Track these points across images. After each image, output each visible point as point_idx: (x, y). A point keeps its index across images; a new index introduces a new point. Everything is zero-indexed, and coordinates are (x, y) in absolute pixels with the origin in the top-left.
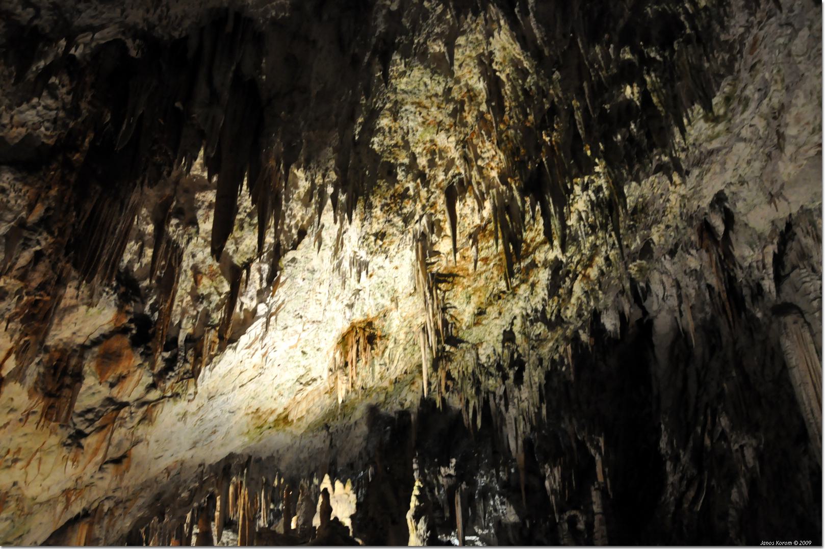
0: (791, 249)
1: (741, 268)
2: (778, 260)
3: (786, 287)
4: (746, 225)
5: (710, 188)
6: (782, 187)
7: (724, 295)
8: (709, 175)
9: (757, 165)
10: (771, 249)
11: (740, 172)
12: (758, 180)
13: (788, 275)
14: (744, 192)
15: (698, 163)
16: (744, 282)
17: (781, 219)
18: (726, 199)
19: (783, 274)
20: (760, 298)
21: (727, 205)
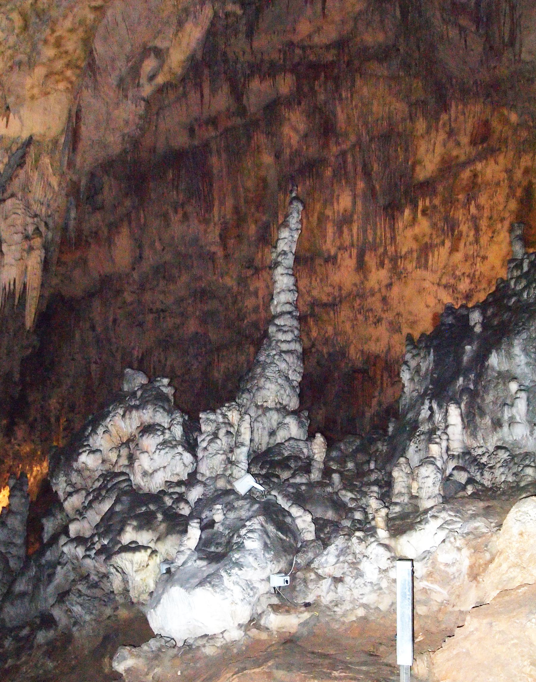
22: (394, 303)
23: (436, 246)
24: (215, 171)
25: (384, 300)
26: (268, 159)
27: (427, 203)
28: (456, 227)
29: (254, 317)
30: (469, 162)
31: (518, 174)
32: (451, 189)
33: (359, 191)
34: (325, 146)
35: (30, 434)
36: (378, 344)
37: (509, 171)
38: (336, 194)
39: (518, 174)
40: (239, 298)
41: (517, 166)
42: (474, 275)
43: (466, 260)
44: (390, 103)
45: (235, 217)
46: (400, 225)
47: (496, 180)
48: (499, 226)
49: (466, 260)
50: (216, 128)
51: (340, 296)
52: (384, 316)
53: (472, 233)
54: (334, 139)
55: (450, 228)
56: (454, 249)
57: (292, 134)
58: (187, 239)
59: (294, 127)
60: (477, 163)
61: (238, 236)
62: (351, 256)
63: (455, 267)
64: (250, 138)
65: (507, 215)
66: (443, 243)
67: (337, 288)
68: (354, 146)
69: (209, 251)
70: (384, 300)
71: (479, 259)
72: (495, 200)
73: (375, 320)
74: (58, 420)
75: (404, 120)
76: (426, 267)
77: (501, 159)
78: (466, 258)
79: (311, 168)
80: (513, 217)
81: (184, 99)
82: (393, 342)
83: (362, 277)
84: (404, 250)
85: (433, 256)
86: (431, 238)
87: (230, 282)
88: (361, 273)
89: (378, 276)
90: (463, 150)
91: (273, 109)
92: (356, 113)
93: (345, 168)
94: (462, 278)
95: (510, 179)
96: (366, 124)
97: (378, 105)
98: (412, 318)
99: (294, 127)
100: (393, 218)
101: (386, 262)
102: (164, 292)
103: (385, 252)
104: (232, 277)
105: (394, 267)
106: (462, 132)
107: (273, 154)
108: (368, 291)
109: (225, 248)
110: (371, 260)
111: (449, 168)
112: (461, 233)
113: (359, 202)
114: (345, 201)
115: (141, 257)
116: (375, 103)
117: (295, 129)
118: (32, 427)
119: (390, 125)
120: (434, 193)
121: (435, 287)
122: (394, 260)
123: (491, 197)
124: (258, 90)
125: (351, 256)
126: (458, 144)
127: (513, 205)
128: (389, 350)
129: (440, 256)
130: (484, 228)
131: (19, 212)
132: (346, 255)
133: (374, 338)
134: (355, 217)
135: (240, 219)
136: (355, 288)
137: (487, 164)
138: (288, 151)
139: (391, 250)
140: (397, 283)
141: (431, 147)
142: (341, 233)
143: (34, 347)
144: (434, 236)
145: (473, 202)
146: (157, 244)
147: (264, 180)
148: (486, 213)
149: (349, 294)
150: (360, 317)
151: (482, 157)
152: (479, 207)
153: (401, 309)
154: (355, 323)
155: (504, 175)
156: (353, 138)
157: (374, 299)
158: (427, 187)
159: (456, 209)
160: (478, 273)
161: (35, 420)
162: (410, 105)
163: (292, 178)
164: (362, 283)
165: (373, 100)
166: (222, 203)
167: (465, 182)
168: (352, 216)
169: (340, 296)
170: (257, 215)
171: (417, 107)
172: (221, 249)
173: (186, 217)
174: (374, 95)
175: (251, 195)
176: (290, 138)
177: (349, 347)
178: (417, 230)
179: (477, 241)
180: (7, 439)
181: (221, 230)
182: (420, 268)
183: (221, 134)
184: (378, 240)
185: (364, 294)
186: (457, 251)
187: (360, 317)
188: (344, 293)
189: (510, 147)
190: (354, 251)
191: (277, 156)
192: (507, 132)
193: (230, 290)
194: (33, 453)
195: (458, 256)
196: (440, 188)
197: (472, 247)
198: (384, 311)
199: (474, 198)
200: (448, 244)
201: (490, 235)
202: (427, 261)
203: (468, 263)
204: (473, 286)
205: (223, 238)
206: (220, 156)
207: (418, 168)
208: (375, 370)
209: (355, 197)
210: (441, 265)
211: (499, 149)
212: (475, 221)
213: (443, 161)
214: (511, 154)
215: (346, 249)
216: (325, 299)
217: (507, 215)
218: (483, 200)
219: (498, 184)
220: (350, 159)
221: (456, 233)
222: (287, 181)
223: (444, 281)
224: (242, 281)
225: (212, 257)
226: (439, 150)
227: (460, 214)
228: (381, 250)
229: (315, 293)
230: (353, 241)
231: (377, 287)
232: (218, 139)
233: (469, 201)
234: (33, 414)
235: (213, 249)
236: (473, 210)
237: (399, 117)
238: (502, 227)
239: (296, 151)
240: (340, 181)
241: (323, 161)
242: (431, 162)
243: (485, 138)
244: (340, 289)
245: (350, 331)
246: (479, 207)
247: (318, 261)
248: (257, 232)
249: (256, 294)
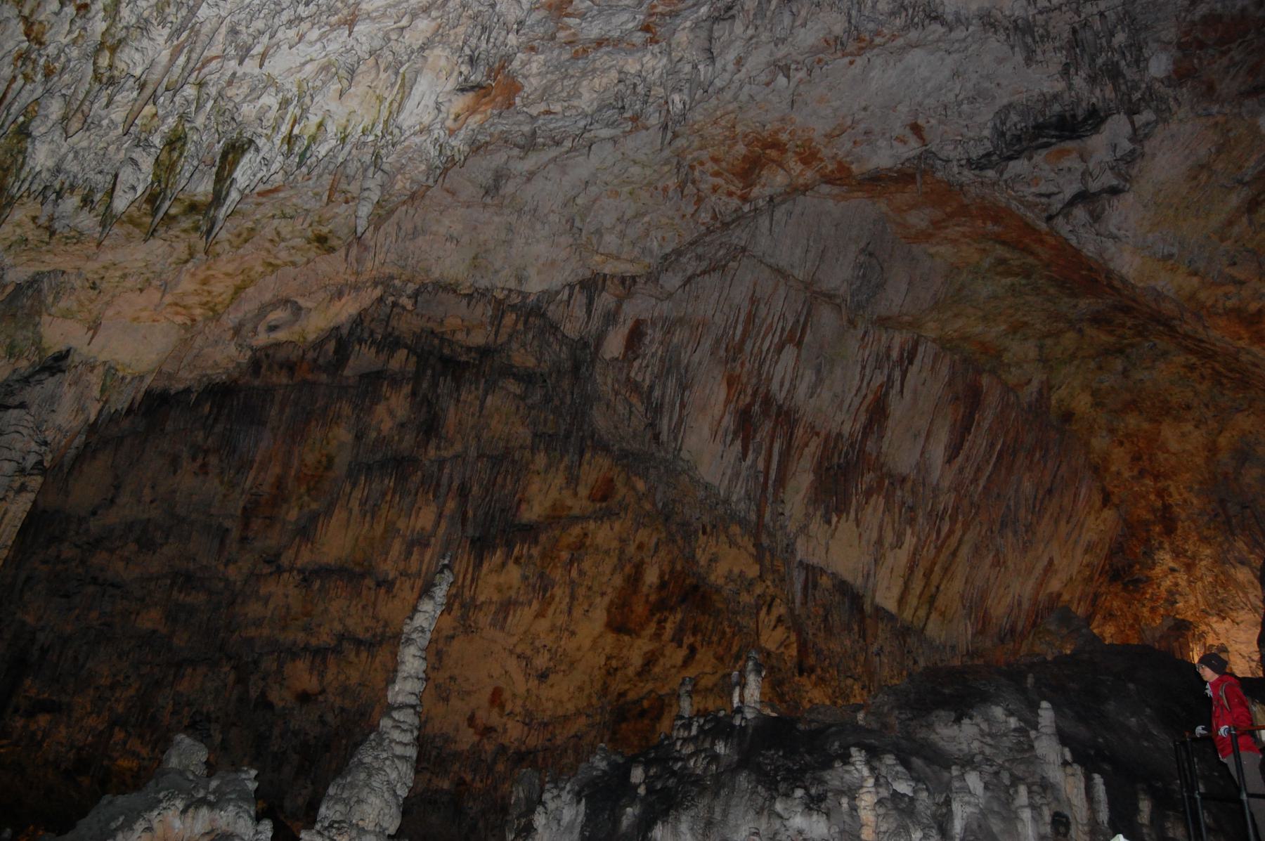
23: (522, 604)
26: (343, 434)
29: (252, 632)
30: (583, 518)
33: (447, 512)
39: (631, 549)
40: (239, 600)
42: (556, 651)
48: (598, 600)
50: (292, 376)
51: (384, 633)
55: (543, 587)
56: (540, 615)
59: (392, 412)
62: (412, 588)
65: (610, 590)
67: (382, 623)
68: (456, 457)
72: (600, 569)
76: (502, 628)
78: (553, 629)
79: (400, 465)
84: (482, 598)
85: (514, 616)
90: (579, 503)
91: (373, 381)
95: (622, 551)
96: (478, 438)
101: (456, 606)
105: (465, 617)
109: (246, 526)
111: (558, 518)
112: (553, 597)
113: (443, 525)
114: (425, 518)
115: (112, 501)
117: (391, 412)
125: (412, 588)
126: (576, 494)
127: (618, 581)
129: (521, 618)
130: (581, 599)
131: (25, 432)
132: (407, 585)
138: (374, 435)
142: (409, 553)
146: (147, 491)
152: (581, 573)
155: (615, 544)
156: (458, 447)
158: (530, 532)
159: (555, 566)
162: (535, 435)
163: (369, 468)
169: (384, 633)
178: (502, 579)
186: (544, 616)
191: (358, 437)
195: (544, 624)
196: (543, 538)
200: (535, 605)
202: (505, 619)
207: (524, 506)
209: (440, 516)
213: (554, 507)
215: (407, 575)
216: (360, 633)
218: (586, 565)
219: (607, 552)
221: (548, 595)
222: (359, 470)
223: (518, 650)
227: (558, 575)
229: (350, 622)
233: (571, 562)
235: (228, 524)
236: (574, 573)
244: (386, 625)
246: (581, 573)
247: (369, 582)
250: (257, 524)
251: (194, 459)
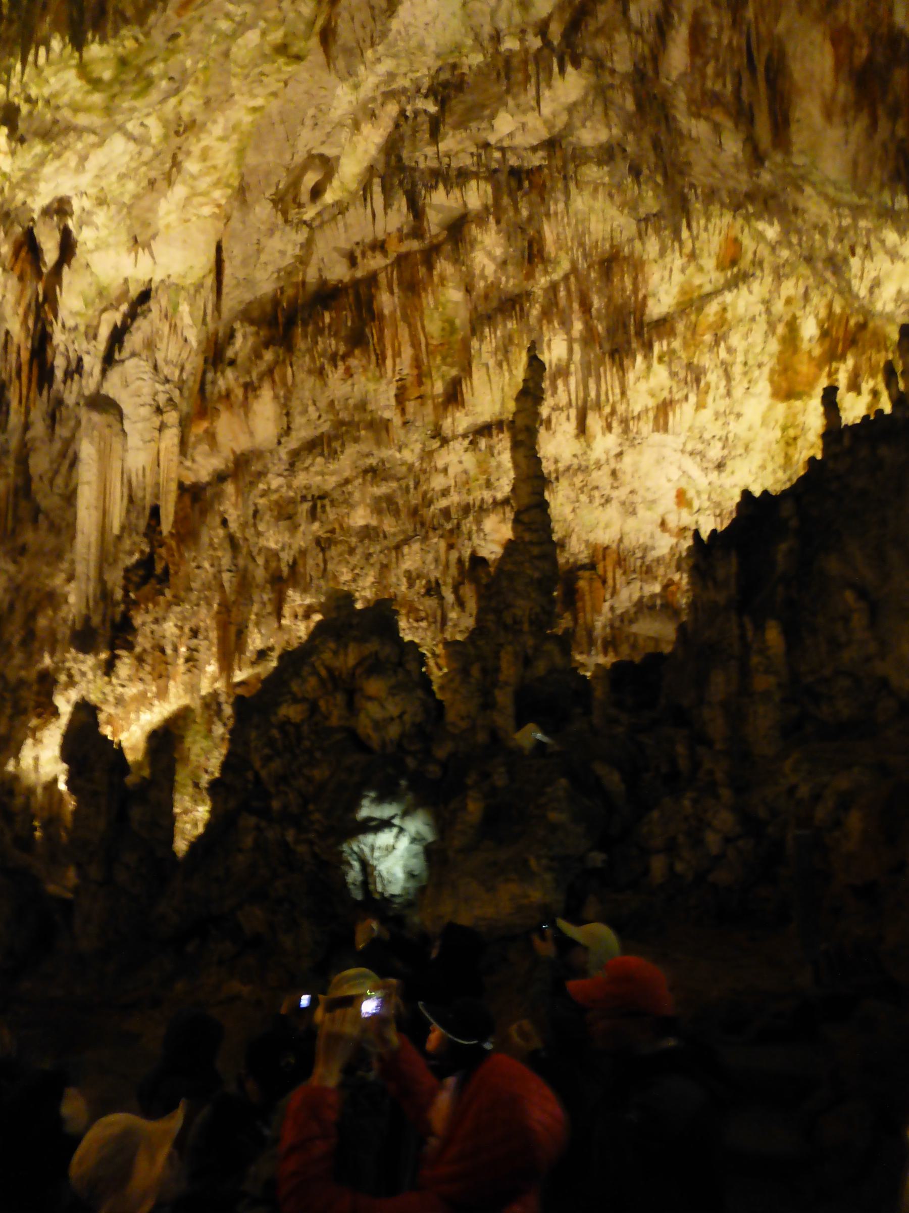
0: (139, 328)
1: (63, 326)
2: (118, 336)
3: (115, 375)
4: (88, 265)
5: (52, 185)
6: (154, 237)
7: (25, 356)
8: (57, 163)
9: (131, 186)
10: (116, 317)
11: (103, 183)
12: (125, 211)
13: (123, 361)
14: (101, 217)
15: (46, 135)
16: (62, 348)
17: (137, 281)
18: (71, 214)
19: (117, 356)
20: (76, 376)
21: (71, 223)
22: (626, 478)
23: (678, 401)
24: (386, 312)
25: (614, 473)
26: (454, 294)
27: (665, 348)
28: (702, 377)
29: (443, 503)
30: (717, 292)
31: (779, 307)
32: (693, 329)
34: (530, 276)
35: (137, 670)
36: (608, 531)
37: (767, 303)
38: (546, 339)
39: (779, 307)
40: (423, 478)
41: (776, 295)
42: (727, 438)
43: (716, 419)
44: (612, 219)
45: (415, 372)
46: (631, 376)
47: (750, 314)
48: (757, 373)
49: (716, 419)
51: (557, 471)
52: (615, 494)
53: (723, 383)
54: (540, 266)
55: (696, 375)
57: (486, 261)
58: (351, 402)
60: (726, 293)
61: (420, 397)
62: (568, 419)
63: (703, 429)
64: (430, 267)
65: (765, 359)
66: (686, 398)
67: (552, 460)
69: (381, 419)
70: (614, 473)
71: (732, 417)
72: (750, 340)
73: (603, 501)
74: (175, 649)
75: (631, 240)
76: (666, 430)
77: (756, 286)
78: (717, 415)
80: (774, 360)
81: (340, 217)
82: (627, 529)
83: (584, 444)
84: (637, 408)
86: (671, 392)
87: (410, 455)
88: (582, 440)
89: (604, 443)
90: (709, 275)
92: (569, 232)
93: (557, 304)
94: (712, 442)
95: (768, 311)
96: (582, 245)
97: (598, 221)
98: (650, 496)
99: (488, 250)
100: (622, 368)
101: (615, 424)
102: (322, 474)
103: (613, 412)
104: (412, 451)
105: (626, 431)
106: (706, 254)
107: (463, 288)
108: (592, 462)
109: (403, 412)
110: (594, 422)
112: (708, 385)
115: (289, 428)
116: (593, 218)
117: (489, 254)
118: (140, 660)
119: (612, 246)
120: (672, 333)
121: (679, 454)
122: (625, 422)
123: (746, 336)
124: (441, 203)
125: (568, 419)
126: (700, 269)
127: (774, 346)
128: (621, 540)
129: (684, 416)
132: (563, 416)
133: (602, 525)
134: (572, 368)
135: (422, 375)
136: (576, 461)
137: (737, 296)
138: (482, 284)
139: (621, 408)
140: (630, 451)
141: (666, 274)
143: (142, 552)
144: (675, 390)
145: (722, 344)
147: (451, 323)
148: (740, 358)
149: (568, 468)
150: (583, 498)
151: (732, 284)
152: (730, 350)
153: (636, 485)
154: (577, 505)
155: (761, 308)
156: (565, 265)
157: (600, 473)
158: (664, 326)
159: (702, 353)
160: (731, 436)
161: (145, 650)
164: (585, 453)
165: (591, 214)
166: (397, 354)
167: (711, 319)
168: (568, 366)
169: (557, 471)
170: (444, 368)
171: (647, 223)
172: (399, 415)
173: (349, 373)
174: (591, 209)
175: (434, 342)
176: (484, 267)
177: (570, 537)
178: (653, 382)
179: (729, 394)
180: (106, 679)
181: (398, 388)
182: (658, 431)
183: (392, 264)
184: (603, 398)
185: (587, 467)
187: (583, 498)
188: (561, 466)
189: (767, 271)
190: (573, 412)
191: (468, 290)
192: (764, 251)
193: (411, 467)
194: (143, 695)
195: (707, 414)
196: (680, 327)
197: (722, 402)
198: (613, 487)
199: (725, 337)
200: (693, 398)
201: (746, 386)
202: (666, 423)
203: (720, 422)
204: (726, 452)
205: (401, 398)
206: (392, 293)
207: (651, 302)
208: (605, 567)
209: (570, 341)
210: (686, 425)
211: (753, 275)
212: (726, 369)
213: (683, 292)
214: (769, 279)
215: (561, 409)
217: (765, 359)
218: (735, 339)
219: (753, 319)
220: (562, 293)
221: (702, 384)
223: (689, 448)
224: (427, 455)
225: (386, 425)
226: (677, 277)
227: (705, 360)
228: (607, 410)
230: (570, 400)
231: (603, 458)
232: (389, 269)
233: (717, 343)
234: (142, 642)
235: (387, 415)
236: (723, 353)
237: (624, 238)
238: (761, 374)
239: (492, 283)
240: (550, 322)
241: (528, 295)
242: (667, 293)
243: (734, 262)
244: (556, 462)
245: (570, 517)
246: (730, 350)
248: (445, 390)
249: (445, 470)
250: (411, 406)
251: (336, 366)
